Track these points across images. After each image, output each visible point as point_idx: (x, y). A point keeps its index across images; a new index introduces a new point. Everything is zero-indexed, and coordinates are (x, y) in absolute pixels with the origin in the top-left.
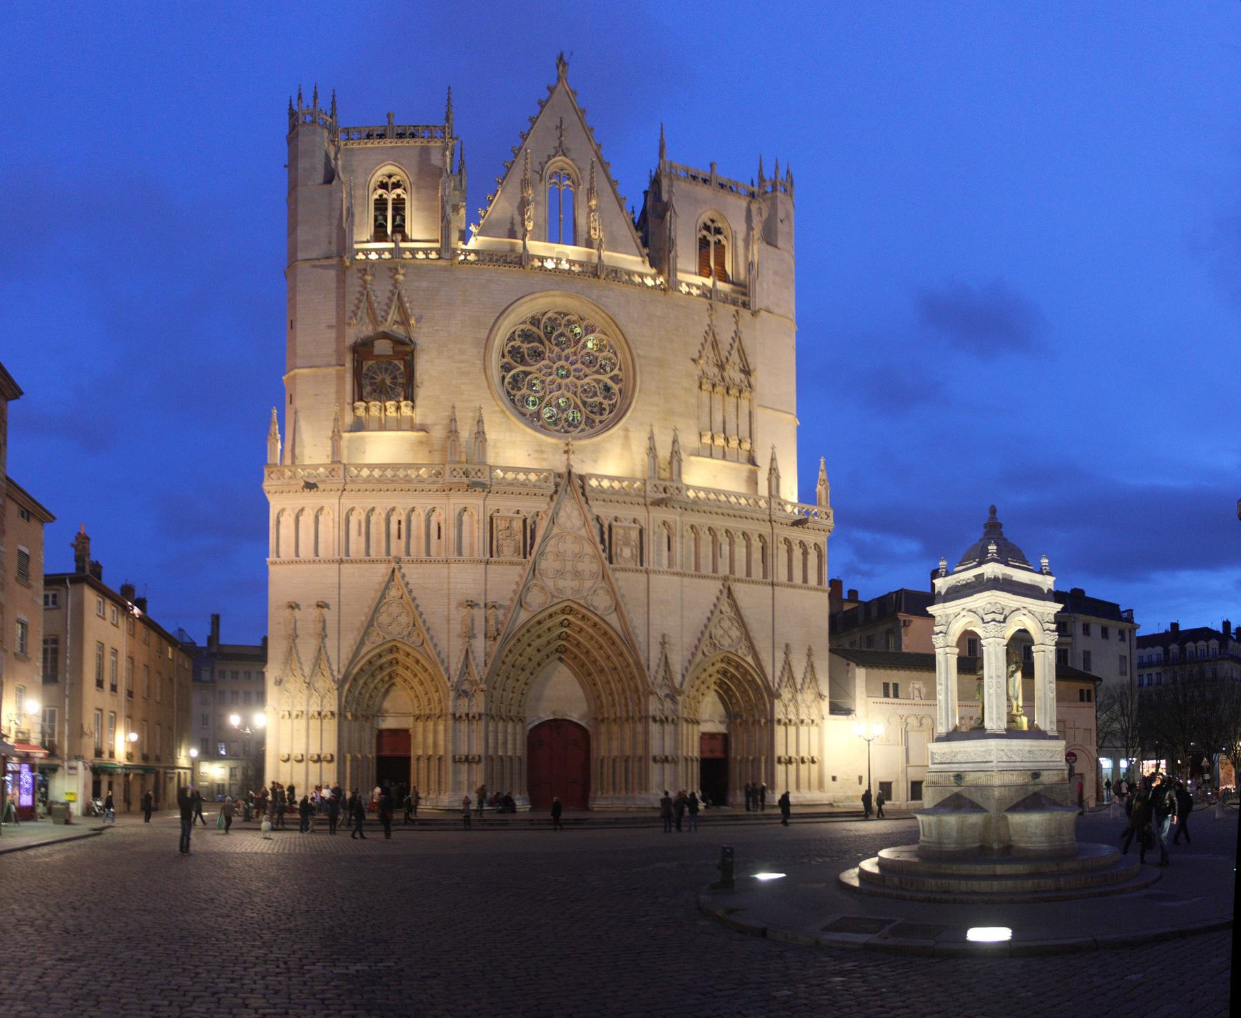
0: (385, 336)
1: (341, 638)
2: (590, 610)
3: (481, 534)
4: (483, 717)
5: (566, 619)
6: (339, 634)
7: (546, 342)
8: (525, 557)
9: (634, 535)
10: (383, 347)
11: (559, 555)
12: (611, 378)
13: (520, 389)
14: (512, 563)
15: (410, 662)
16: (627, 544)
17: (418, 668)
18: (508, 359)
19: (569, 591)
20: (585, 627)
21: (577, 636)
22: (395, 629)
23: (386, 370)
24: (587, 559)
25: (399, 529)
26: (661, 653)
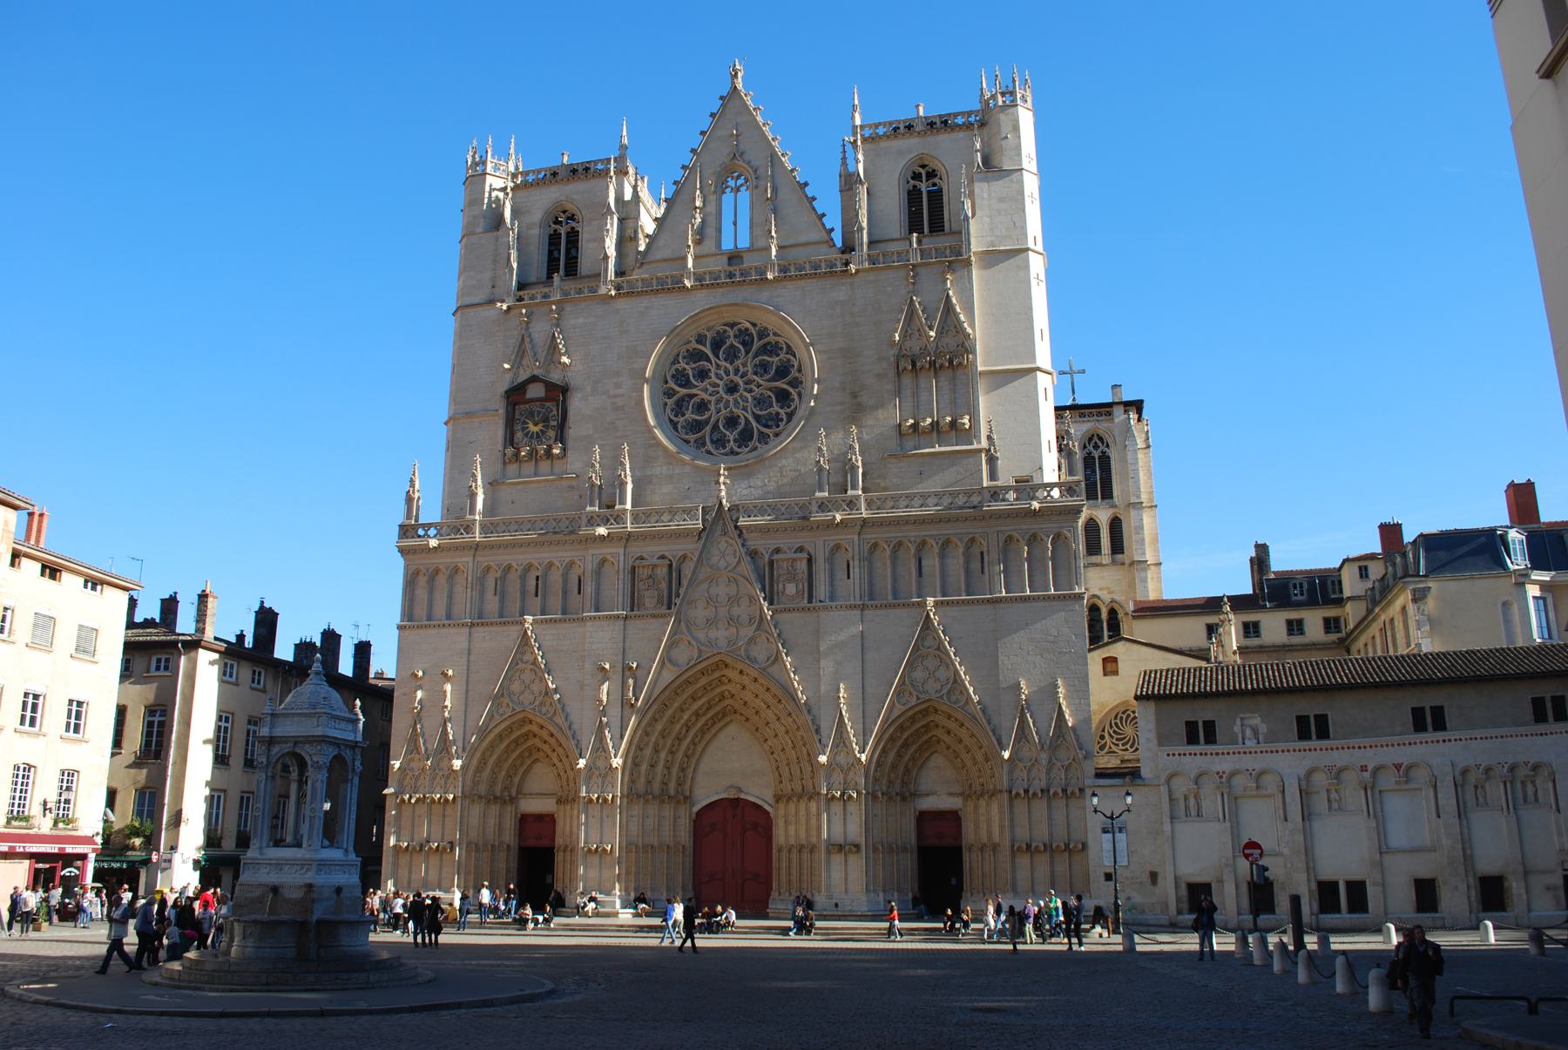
0: (534, 379)
1: (469, 710)
3: (621, 586)
5: (724, 676)
6: (466, 705)
9: (803, 565)
10: (536, 391)
11: (711, 601)
14: (654, 616)
15: (544, 734)
16: (793, 578)
17: (552, 741)
18: (672, 384)
19: (723, 643)
22: (527, 698)
25: (537, 584)
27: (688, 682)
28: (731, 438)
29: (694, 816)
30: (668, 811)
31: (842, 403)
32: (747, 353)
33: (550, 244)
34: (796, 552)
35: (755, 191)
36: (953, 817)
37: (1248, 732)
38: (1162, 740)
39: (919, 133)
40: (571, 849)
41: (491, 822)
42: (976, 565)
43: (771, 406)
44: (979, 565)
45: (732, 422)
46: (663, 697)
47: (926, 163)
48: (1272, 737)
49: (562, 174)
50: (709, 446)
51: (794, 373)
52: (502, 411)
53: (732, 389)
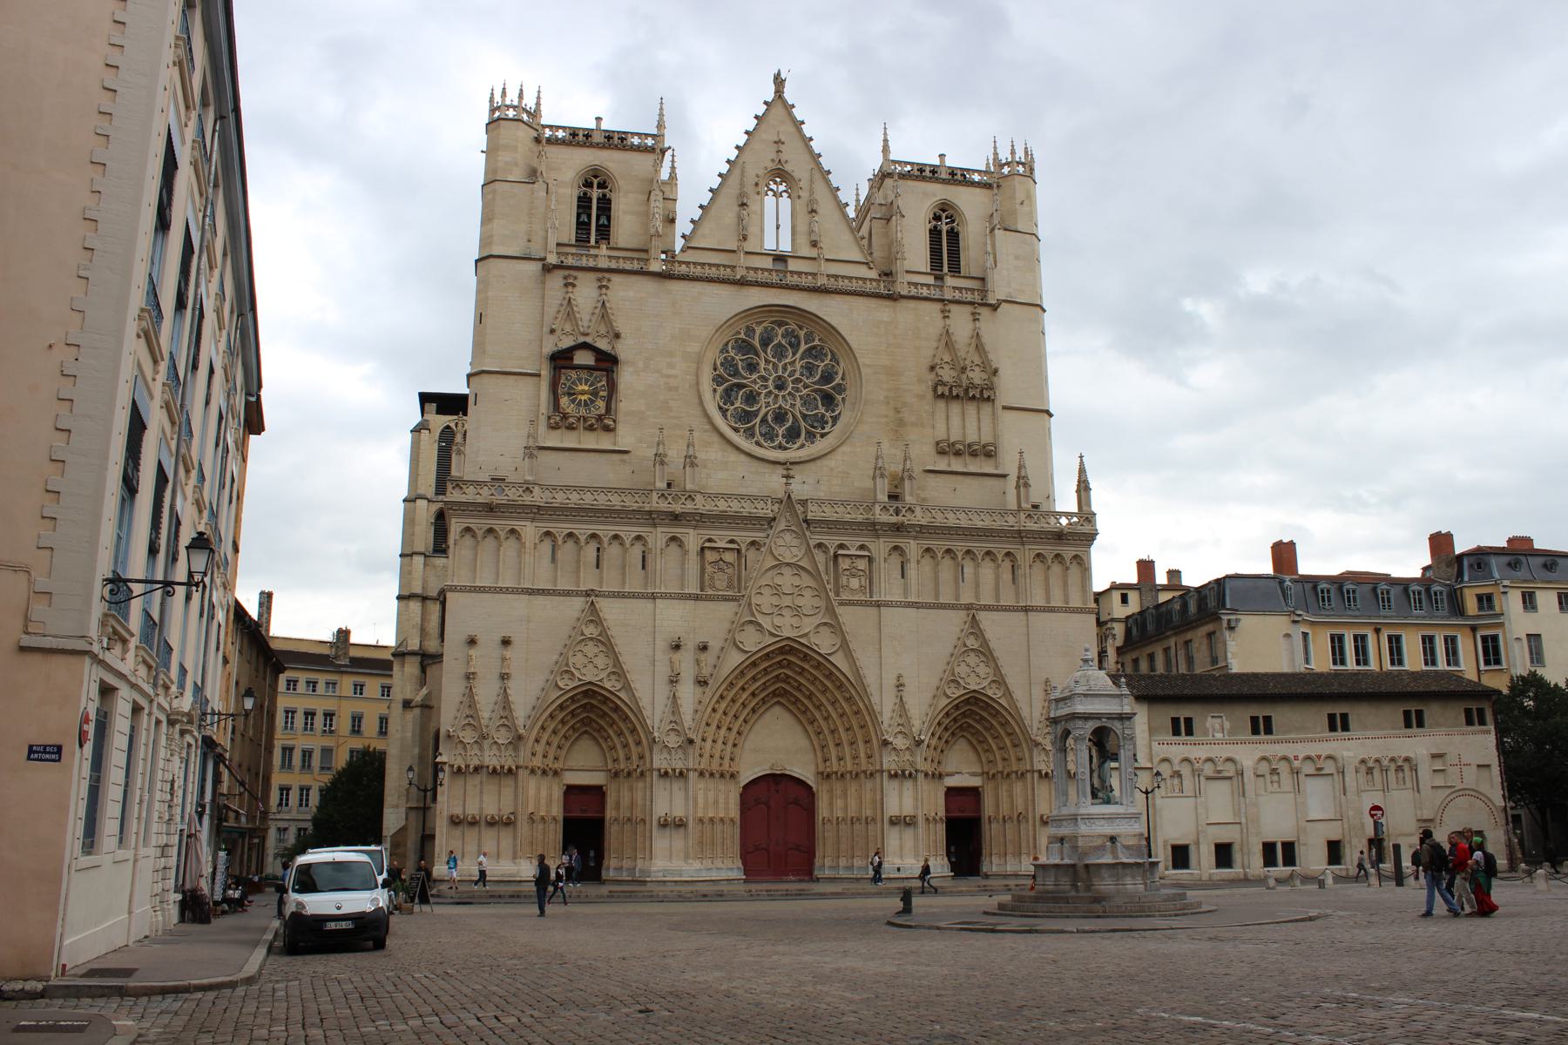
7: (763, 354)
9: (862, 564)
10: (584, 358)
11: (777, 591)
12: (833, 388)
13: (732, 404)
14: (726, 599)
18: (721, 370)
20: (807, 667)
23: (587, 381)
24: (808, 593)
25: (598, 556)
27: (754, 664)
28: (780, 432)
30: (722, 785)
31: (887, 416)
32: (794, 354)
33: (579, 207)
35: (798, 201)
36: (974, 792)
37: (1217, 726)
38: (1152, 731)
39: (944, 180)
40: (637, 823)
41: (544, 793)
42: (1006, 576)
43: (817, 408)
44: (1010, 576)
45: (780, 417)
46: (732, 676)
47: (946, 208)
48: (1232, 732)
49: (598, 138)
50: (758, 437)
51: (838, 380)
52: (546, 372)
53: (780, 387)
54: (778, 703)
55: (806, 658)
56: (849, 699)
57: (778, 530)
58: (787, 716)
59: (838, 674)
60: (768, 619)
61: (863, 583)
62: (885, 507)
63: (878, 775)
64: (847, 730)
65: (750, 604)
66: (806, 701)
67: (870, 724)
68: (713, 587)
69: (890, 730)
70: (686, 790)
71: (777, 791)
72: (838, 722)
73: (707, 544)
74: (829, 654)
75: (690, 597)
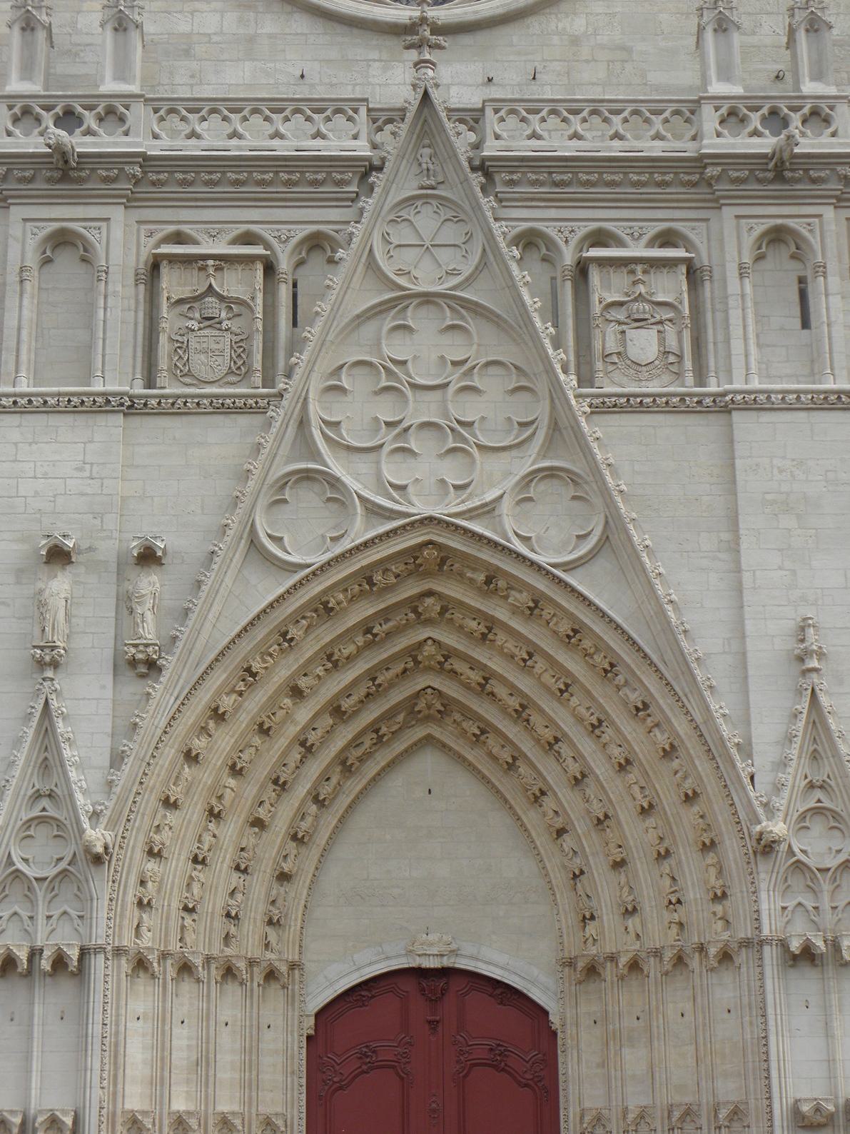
2: (511, 551)
4: (98, 964)
5: (430, 593)
8: (268, 381)
9: (669, 288)
14: (223, 407)
20: (501, 614)
21: (480, 654)
24: (494, 385)
26: (799, 692)
27: (324, 609)
29: (312, 1021)
34: (651, 244)
46: (246, 646)
54: (429, 740)
55: (491, 583)
56: (641, 710)
57: (395, 196)
58: (463, 785)
59: (598, 627)
60: (363, 465)
61: (672, 342)
62: (732, 113)
63: (742, 957)
64: (645, 811)
65: (303, 423)
66: (512, 730)
67: (711, 787)
68: (184, 373)
69: (780, 802)
70: (82, 1018)
71: (433, 1024)
72: (614, 786)
73: (166, 249)
74: (568, 567)
75: (104, 405)
